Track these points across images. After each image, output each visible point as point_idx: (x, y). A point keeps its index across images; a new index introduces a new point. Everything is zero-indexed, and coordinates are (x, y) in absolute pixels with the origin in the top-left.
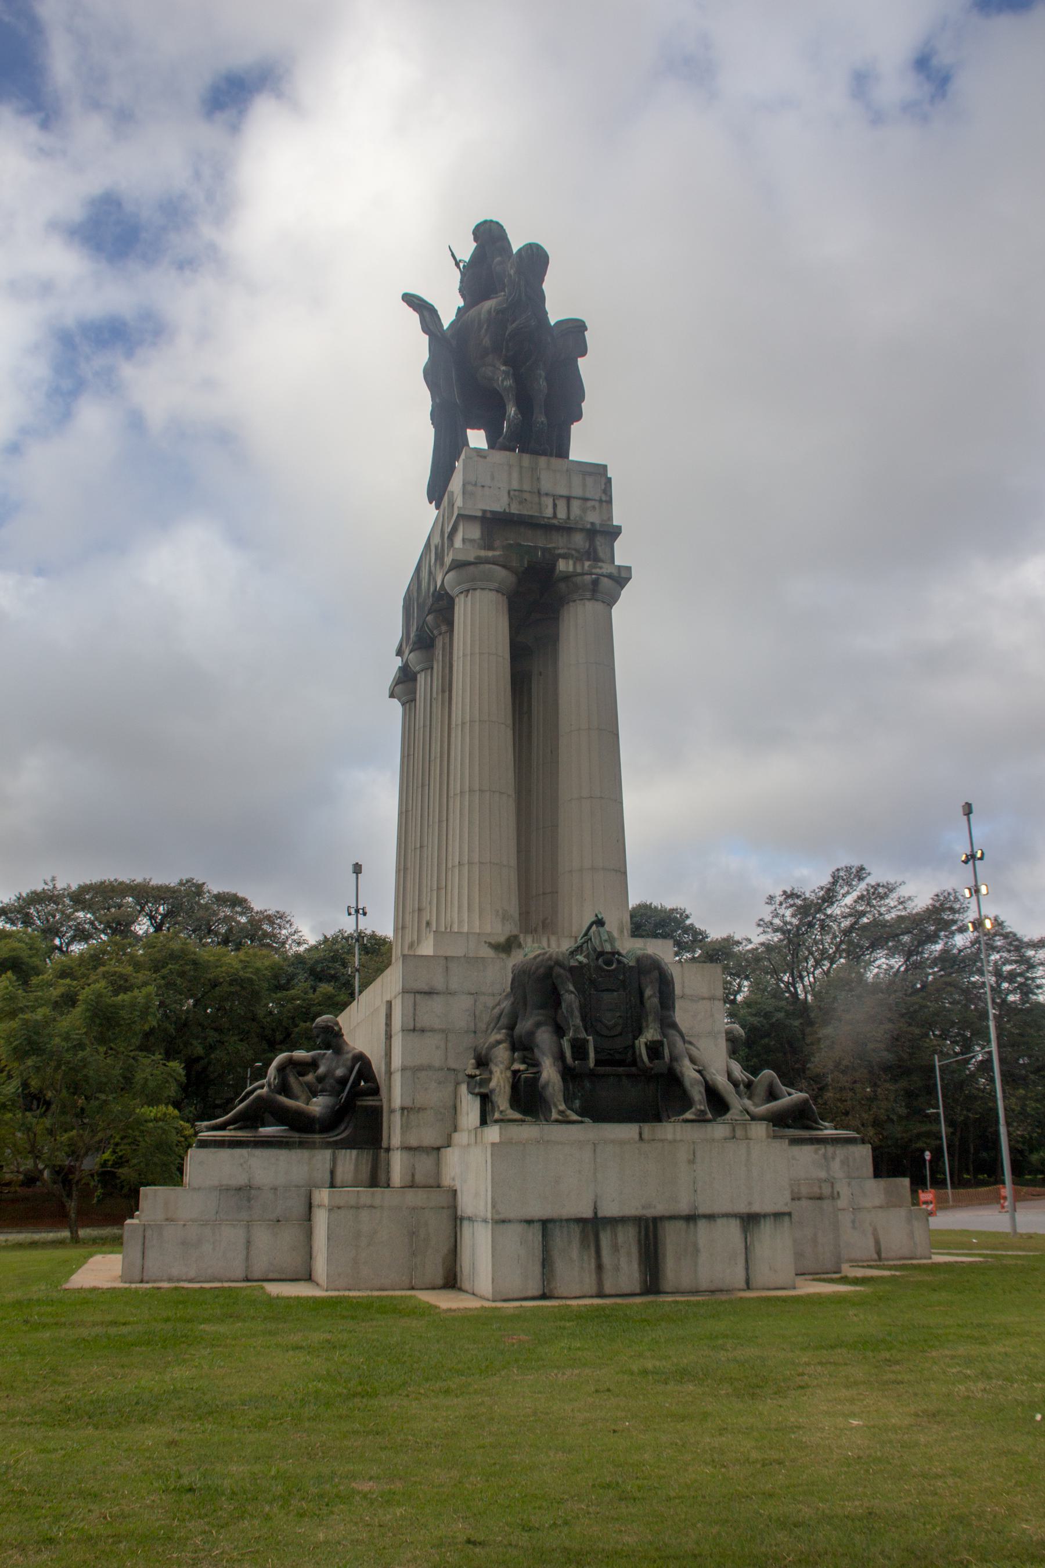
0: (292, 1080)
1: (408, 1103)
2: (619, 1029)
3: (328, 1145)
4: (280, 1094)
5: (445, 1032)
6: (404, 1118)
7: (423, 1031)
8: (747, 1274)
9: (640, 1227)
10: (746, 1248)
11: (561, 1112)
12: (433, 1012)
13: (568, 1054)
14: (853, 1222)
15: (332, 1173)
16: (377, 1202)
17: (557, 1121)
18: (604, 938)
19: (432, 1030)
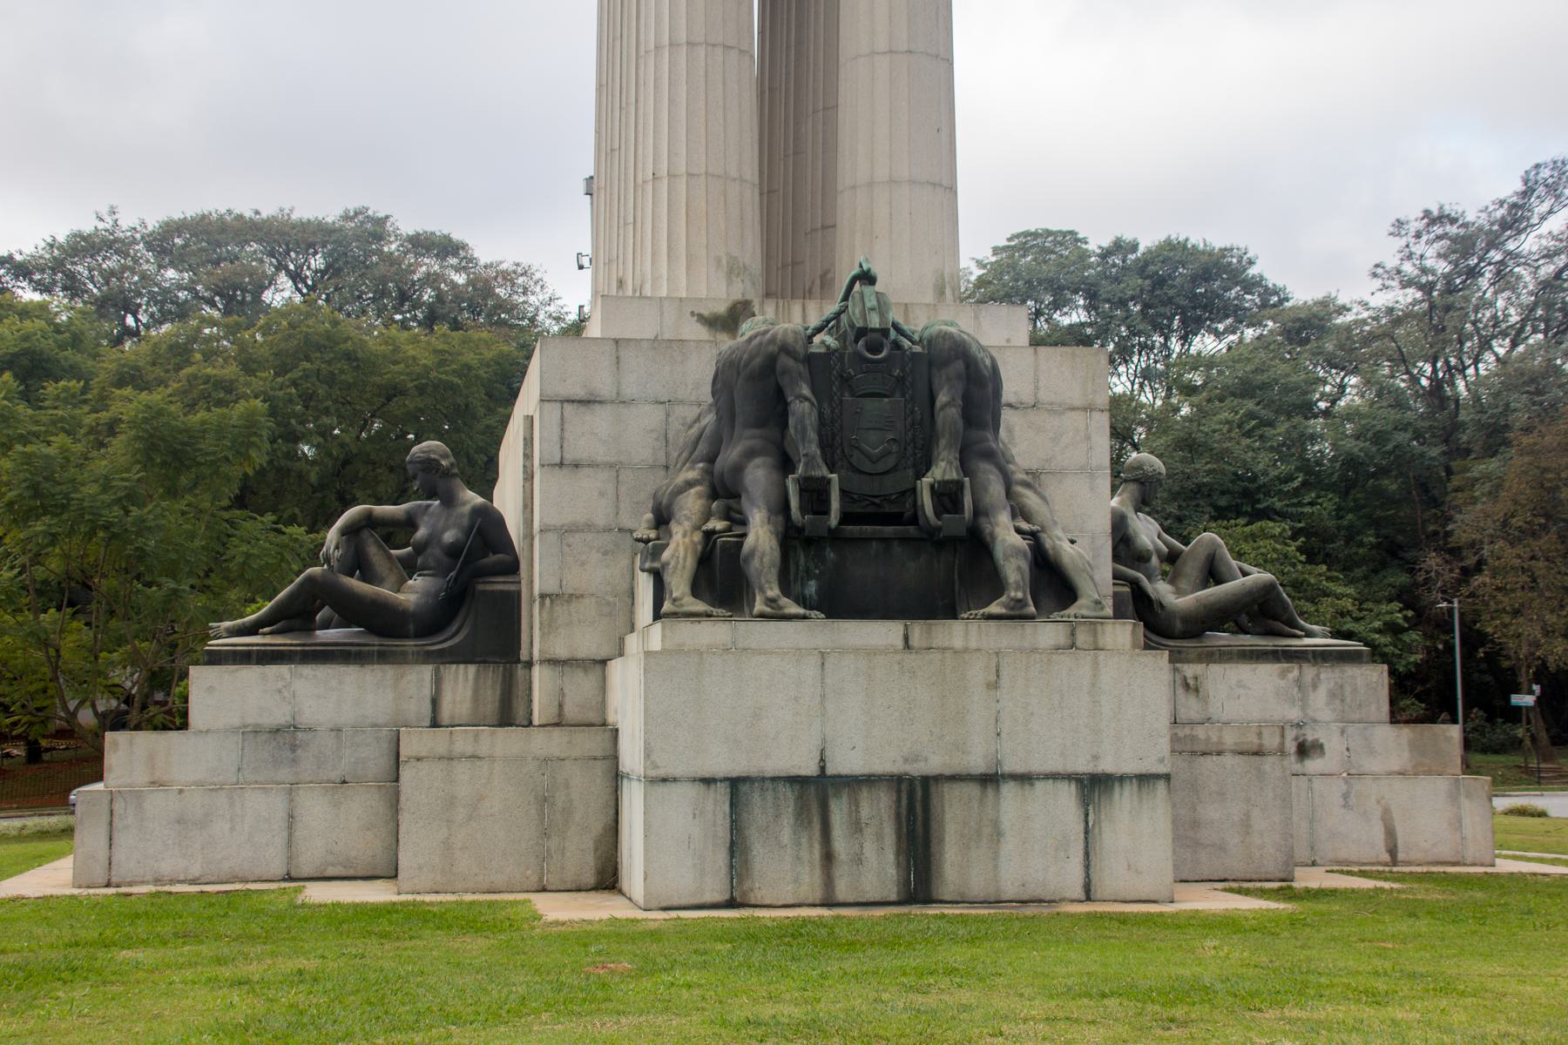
0: (373, 552)
1: (551, 587)
2: (890, 462)
3: (427, 657)
4: (352, 575)
5: (615, 467)
6: (545, 615)
7: (577, 466)
8: (1088, 876)
9: (899, 791)
10: (1087, 832)
11: (771, 601)
12: (593, 434)
13: (794, 503)
14: (1346, 796)
15: (435, 702)
16: (483, 749)
17: (762, 616)
18: (868, 305)
19: (593, 465)
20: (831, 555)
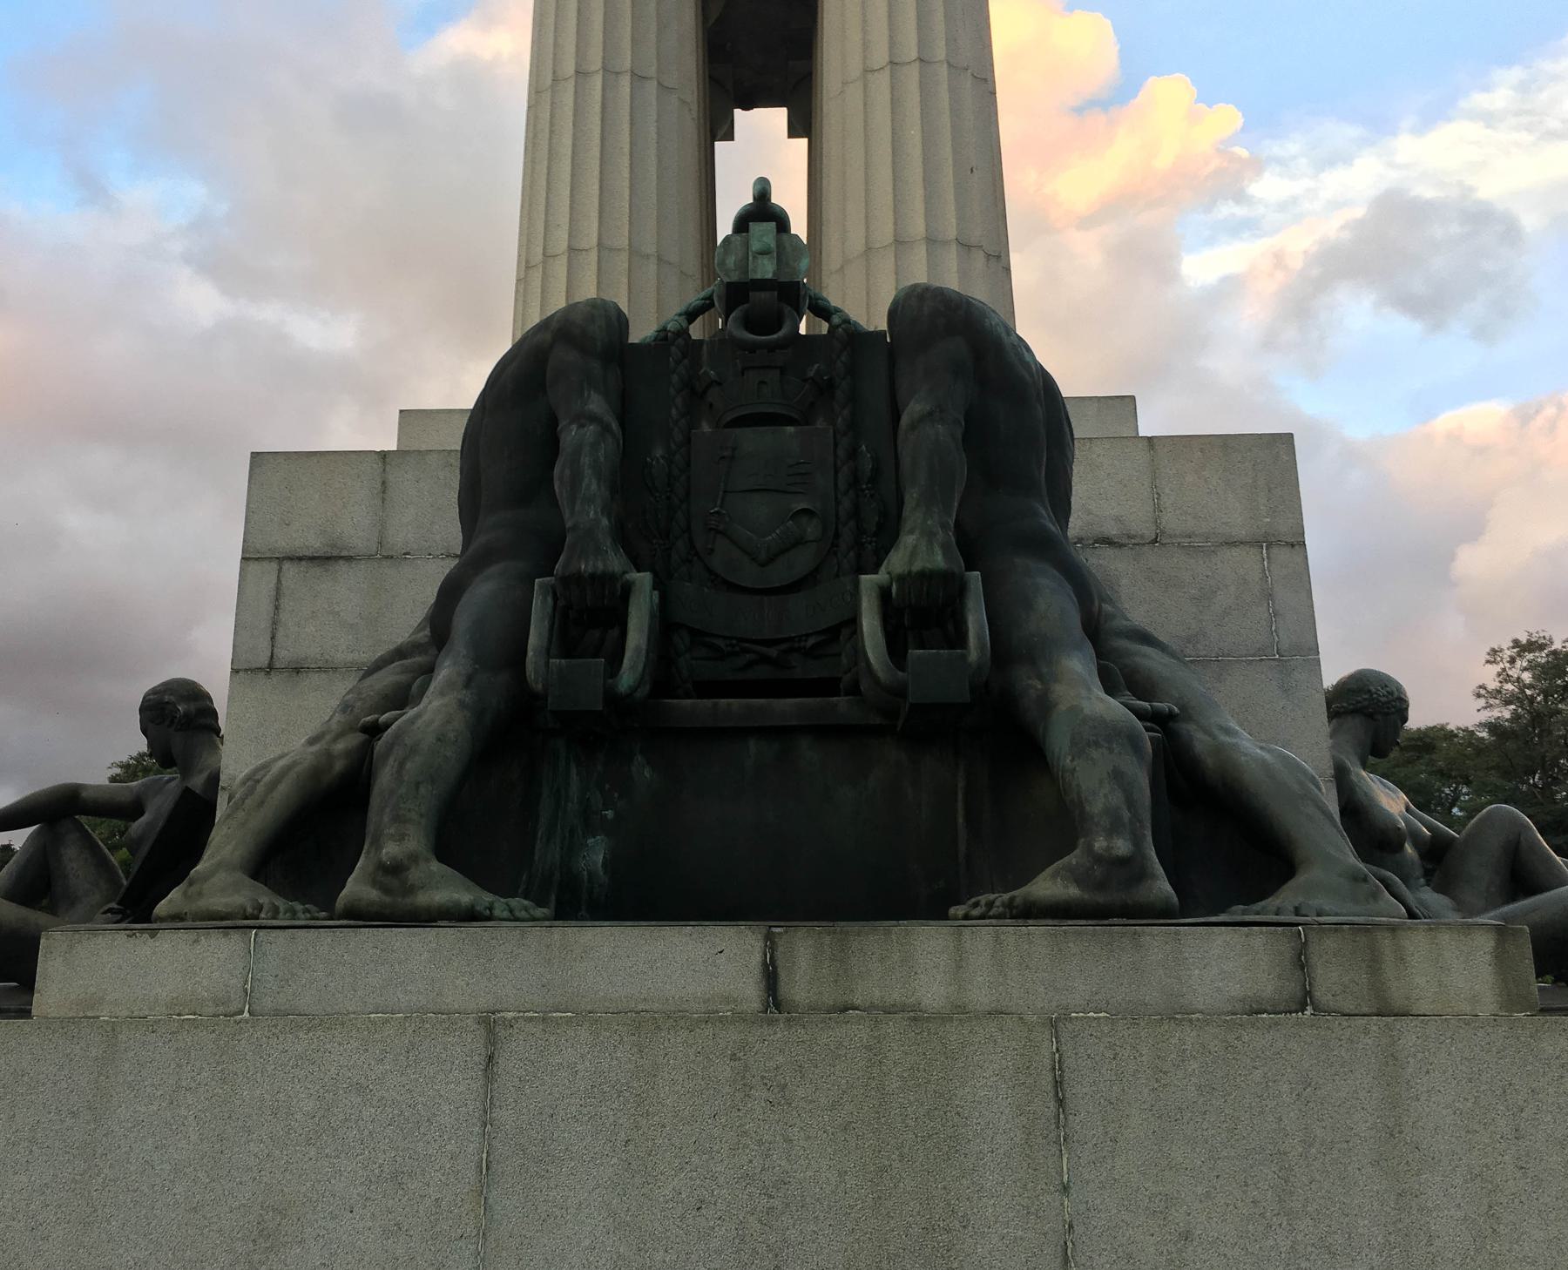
2: (801, 561)
7: (297, 670)
20: (643, 772)
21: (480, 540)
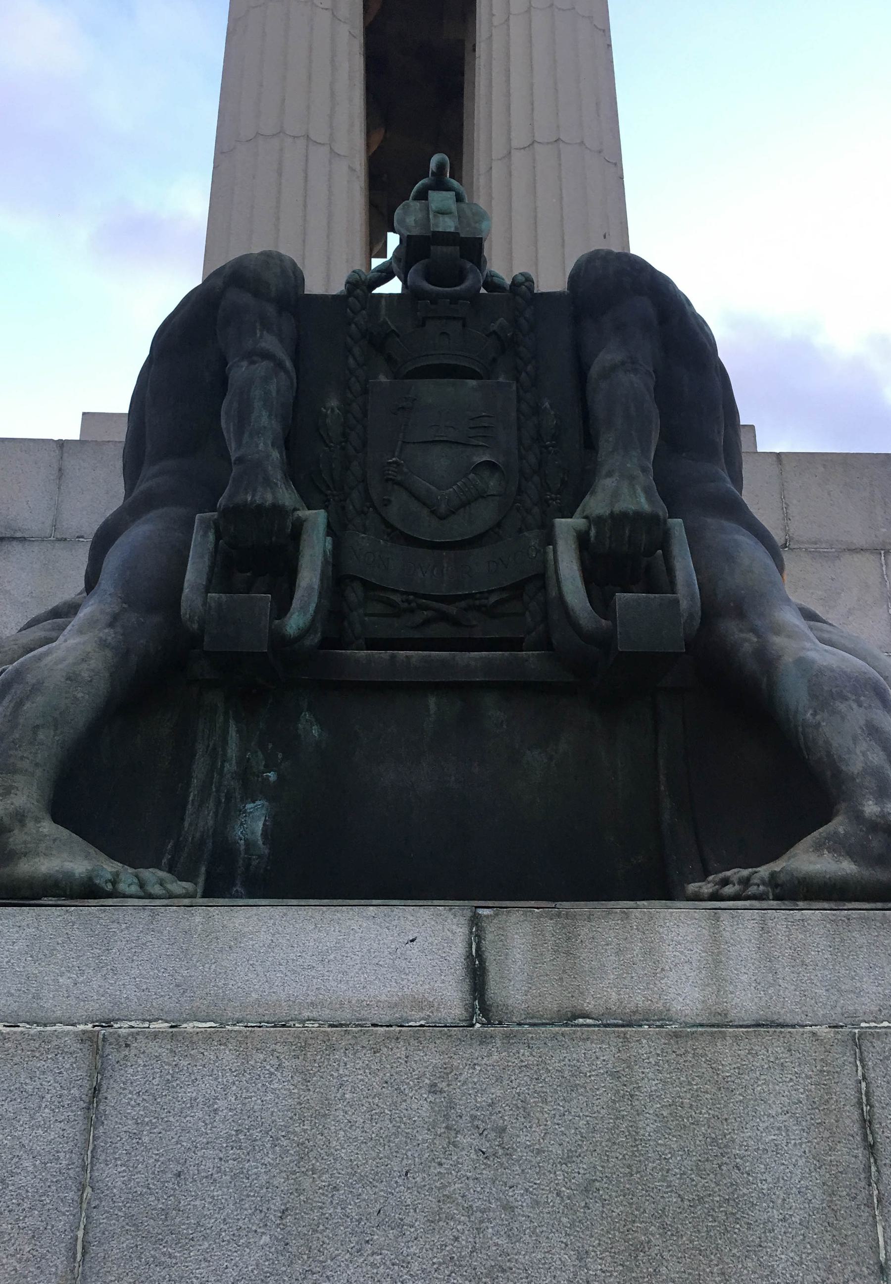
2: (484, 515)
13: (194, 574)
21: (142, 487)
